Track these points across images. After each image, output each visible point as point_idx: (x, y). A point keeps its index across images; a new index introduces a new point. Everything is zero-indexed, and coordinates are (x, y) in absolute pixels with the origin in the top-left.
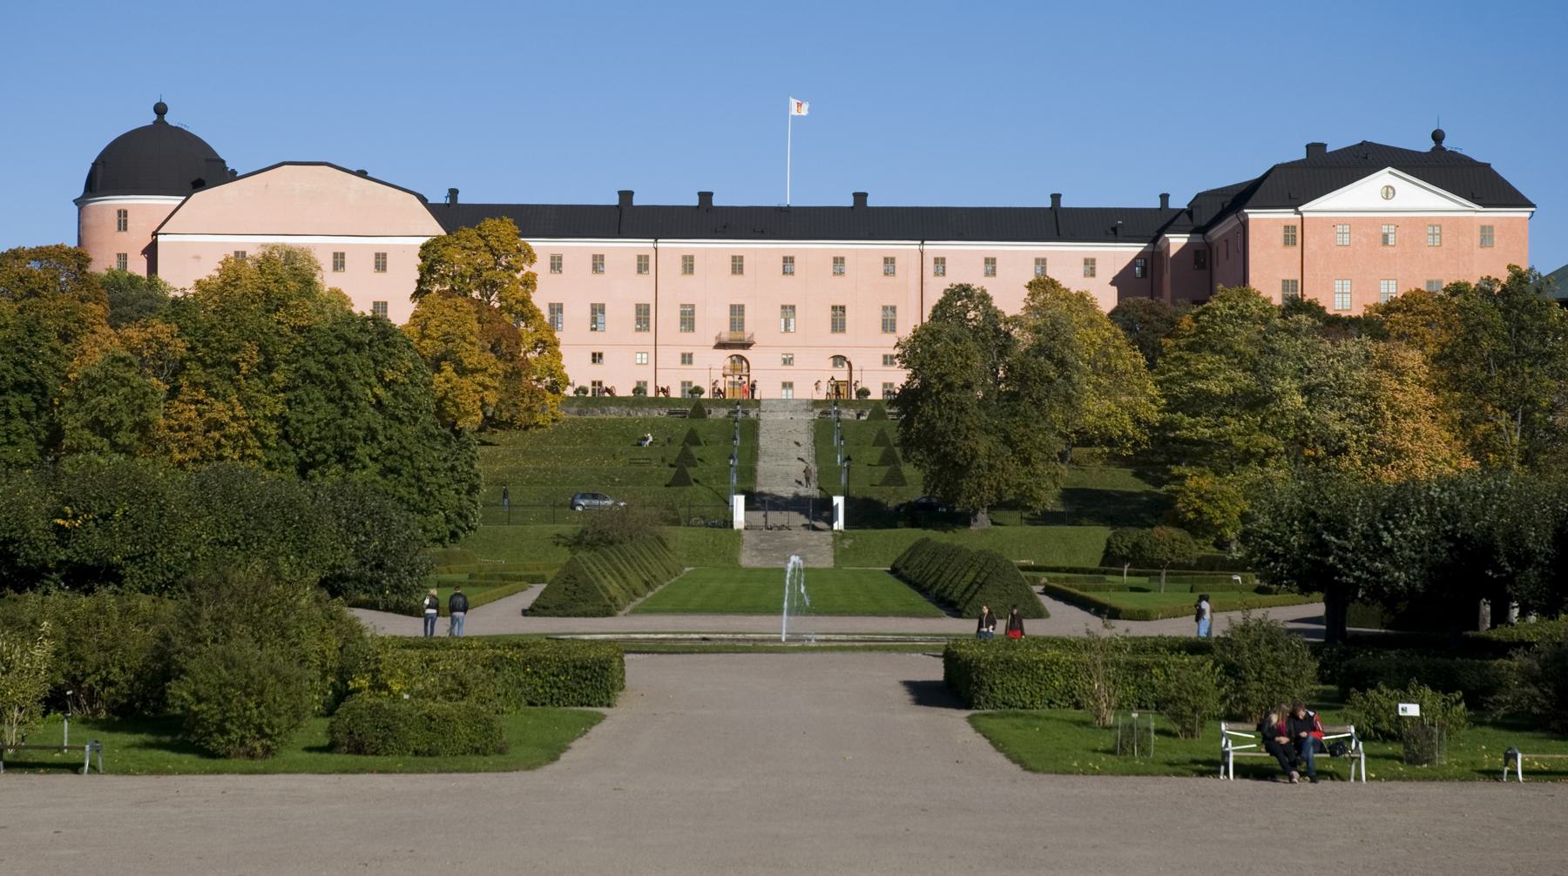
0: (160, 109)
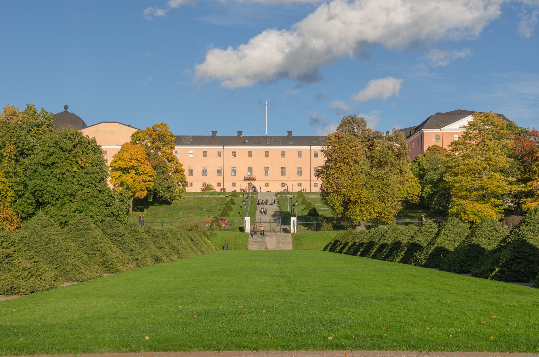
0: (66, 107)
